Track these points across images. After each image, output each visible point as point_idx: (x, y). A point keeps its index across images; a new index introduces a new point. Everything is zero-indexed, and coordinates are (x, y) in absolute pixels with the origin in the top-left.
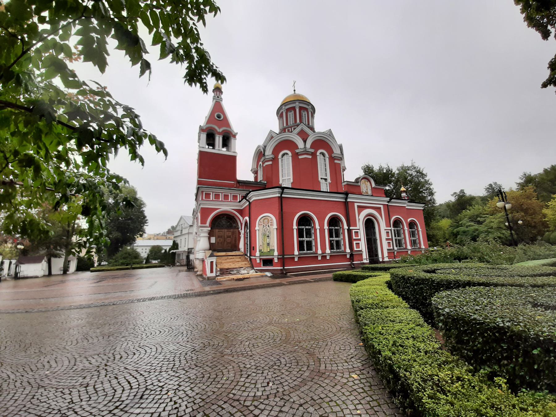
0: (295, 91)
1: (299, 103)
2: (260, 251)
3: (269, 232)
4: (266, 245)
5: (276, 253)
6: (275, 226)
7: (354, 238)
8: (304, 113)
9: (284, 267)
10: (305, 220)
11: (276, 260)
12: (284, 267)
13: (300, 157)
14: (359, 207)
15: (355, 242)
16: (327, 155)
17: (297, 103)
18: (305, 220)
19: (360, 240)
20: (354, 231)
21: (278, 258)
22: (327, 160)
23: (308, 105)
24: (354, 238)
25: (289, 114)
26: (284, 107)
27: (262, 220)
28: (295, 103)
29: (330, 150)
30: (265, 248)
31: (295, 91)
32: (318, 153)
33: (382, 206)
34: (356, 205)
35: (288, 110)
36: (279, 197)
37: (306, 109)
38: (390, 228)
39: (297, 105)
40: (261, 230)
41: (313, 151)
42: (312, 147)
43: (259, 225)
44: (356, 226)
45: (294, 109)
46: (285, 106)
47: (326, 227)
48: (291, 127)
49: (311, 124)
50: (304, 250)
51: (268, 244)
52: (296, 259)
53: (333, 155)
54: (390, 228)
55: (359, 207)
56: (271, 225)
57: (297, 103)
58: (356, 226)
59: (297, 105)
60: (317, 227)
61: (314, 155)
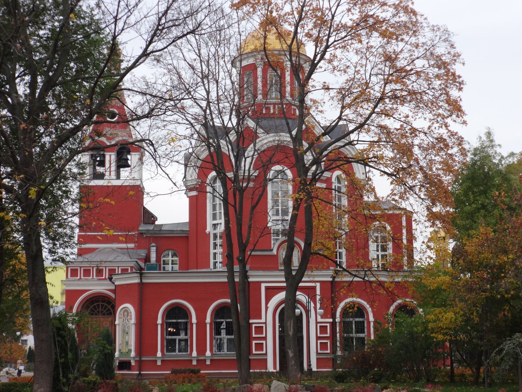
2: (120, 350)
3: (128, 327)
4: (125, 344)
5: (133, 354)
6: (133, 321)
7: (254, 335)
9: (140, 370)
10: (177, 313)
11: (133, 363)
12: (140, 372)
14: (267, 288)
15: (254, 342)
18: (177, 313)
19: (265, 338)
20: (254, 326)
21: (136, 361)
24: (254, 335)
27: (122, 312)
30: (124, 347)
33: (318, 285)
34: (263, 286)
36: (138, 283)
38: (331, 320)
40: (121, 324)
43: (120, 318)
44: (261, 318)
47: (208, 320)
50: (174, 351)
51: (127, 343)
52: (208, 362)
54: (331, 320)
55: (267, 288)
56: (131, 319)
58: (261, 318)
60: (194, 320)
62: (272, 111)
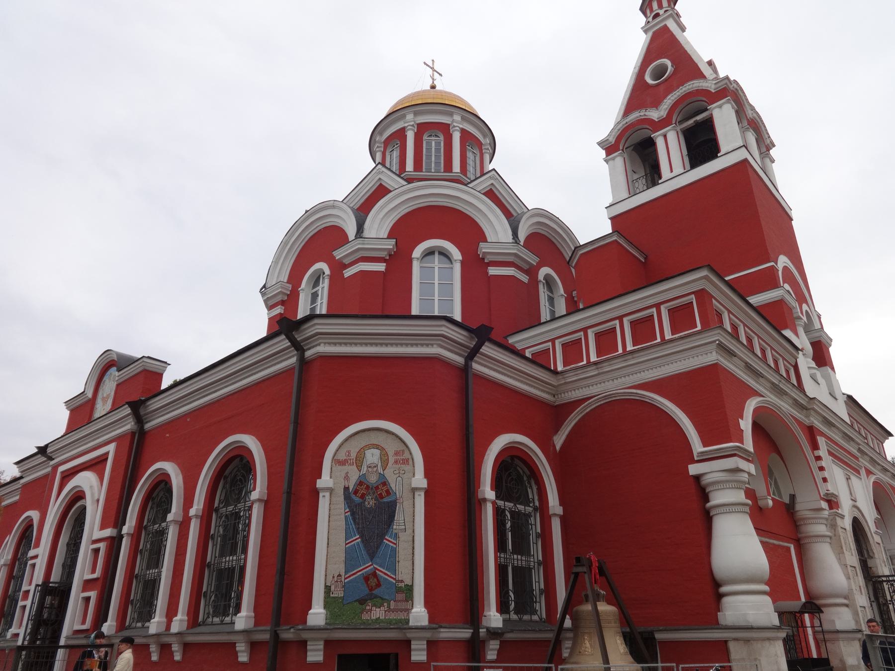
1: (416, 114)
13: (348, 273)
17: (410, 117)
22: (457, 268)
23: (451, 114)
28: (404, 116)
32: (417, 252)
37: (445, 129)
39: (410, 121)
45: (401, 135)
46: (381, 134)
61: (399, 262)
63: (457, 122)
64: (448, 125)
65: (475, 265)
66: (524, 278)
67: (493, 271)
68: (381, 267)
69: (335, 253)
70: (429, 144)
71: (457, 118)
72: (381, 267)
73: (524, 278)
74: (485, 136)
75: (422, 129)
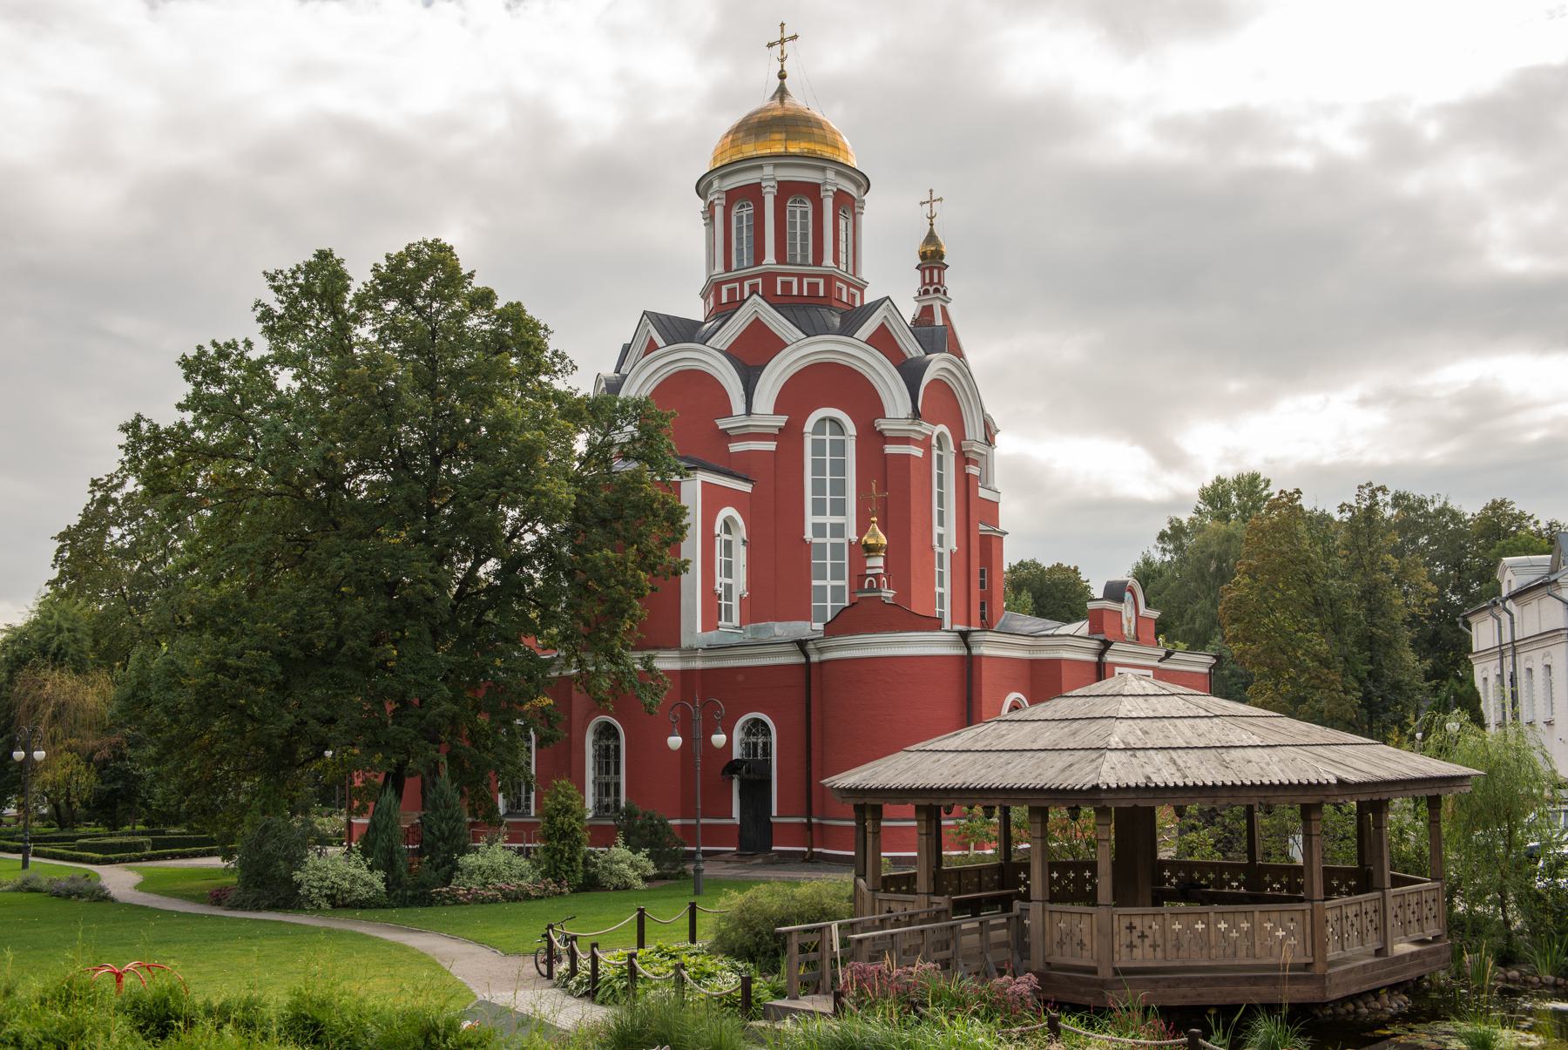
0: (782, 76)
1: (776, 166)
8: (799, 211)
16: (851, 428)
17: (768, 171)
23: (823, 169)
25: (735, 210)
26: (716, 184)
28: (761, 167)
29: (865, 403)
31: (782, 76)
32: (809, 426)
35: (732, 196)
37: (812, 192)
39: (769, 178)
41: (781, 421)
42: (778, 410)
45: (753, 193)
46: (722, 177)
48: (741, 280)
49: (828, 261)
53: (882, 424)
57: (768, 171)
59: (769, 178)
61: (790, 436)
62: (795, 292)
63: (832, 182)
64: (818, 185)
65: (871, 439)
66: (917, 452)
67: (890, 449)
68: (771, 446)
69: (718, 422)
70: (793, 214)
71: (830, 175)
72: (771, 446)
73: (917, 452)
74: (859, 186)
75: (787, 190)
